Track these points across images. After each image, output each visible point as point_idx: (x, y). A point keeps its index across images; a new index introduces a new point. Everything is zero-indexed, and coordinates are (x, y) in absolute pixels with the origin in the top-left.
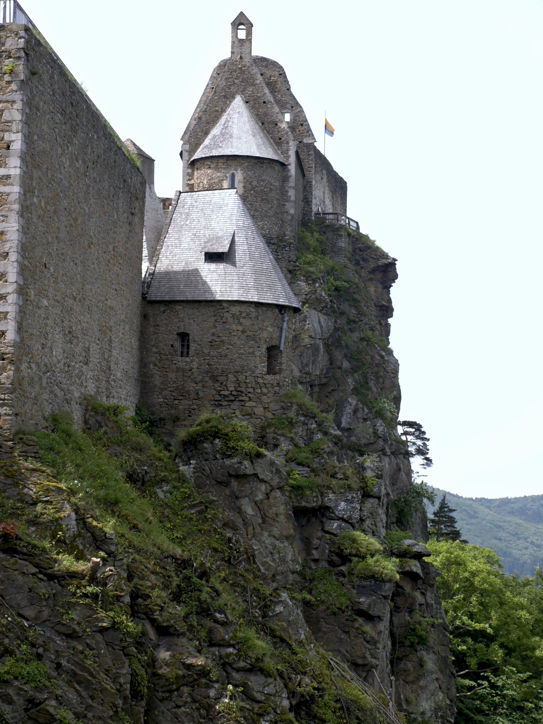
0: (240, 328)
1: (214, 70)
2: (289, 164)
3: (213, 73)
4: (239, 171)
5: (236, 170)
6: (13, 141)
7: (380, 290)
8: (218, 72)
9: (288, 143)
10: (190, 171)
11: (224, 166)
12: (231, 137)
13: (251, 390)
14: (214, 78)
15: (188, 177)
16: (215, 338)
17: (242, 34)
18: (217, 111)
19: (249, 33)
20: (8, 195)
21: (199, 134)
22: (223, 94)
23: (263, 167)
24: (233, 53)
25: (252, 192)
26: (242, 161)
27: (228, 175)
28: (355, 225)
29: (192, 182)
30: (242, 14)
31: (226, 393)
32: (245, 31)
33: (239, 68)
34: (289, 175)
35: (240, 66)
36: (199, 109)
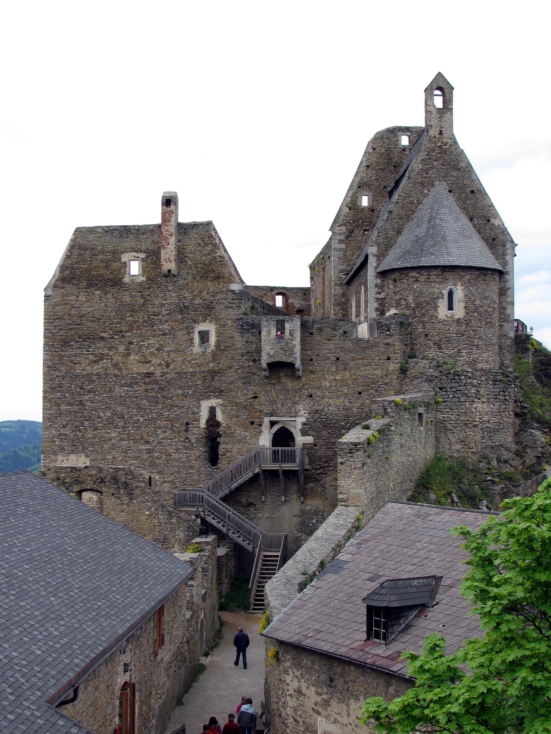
1: (369, 143)
3: (367, 148)
4: (459, 287)
5: (455, 285)
8: (374, 147)
9: (504, 245)
10: (379, 281)
11: (439, 280)
12: (444, 239)
14: (369, 153)
17: (438, 102)
18: (412, 203)
21: (391, 232)
22: (420, 180)
23: (485, 280)
25: (475, 314)
26: (462, 274)
27: (444, 292)
29: (382, 295)
30: (440, 75)
32: (441, 98)
33: (439, 147)
34: (507, 286)
35: (439, 144)
36: (351, 192)
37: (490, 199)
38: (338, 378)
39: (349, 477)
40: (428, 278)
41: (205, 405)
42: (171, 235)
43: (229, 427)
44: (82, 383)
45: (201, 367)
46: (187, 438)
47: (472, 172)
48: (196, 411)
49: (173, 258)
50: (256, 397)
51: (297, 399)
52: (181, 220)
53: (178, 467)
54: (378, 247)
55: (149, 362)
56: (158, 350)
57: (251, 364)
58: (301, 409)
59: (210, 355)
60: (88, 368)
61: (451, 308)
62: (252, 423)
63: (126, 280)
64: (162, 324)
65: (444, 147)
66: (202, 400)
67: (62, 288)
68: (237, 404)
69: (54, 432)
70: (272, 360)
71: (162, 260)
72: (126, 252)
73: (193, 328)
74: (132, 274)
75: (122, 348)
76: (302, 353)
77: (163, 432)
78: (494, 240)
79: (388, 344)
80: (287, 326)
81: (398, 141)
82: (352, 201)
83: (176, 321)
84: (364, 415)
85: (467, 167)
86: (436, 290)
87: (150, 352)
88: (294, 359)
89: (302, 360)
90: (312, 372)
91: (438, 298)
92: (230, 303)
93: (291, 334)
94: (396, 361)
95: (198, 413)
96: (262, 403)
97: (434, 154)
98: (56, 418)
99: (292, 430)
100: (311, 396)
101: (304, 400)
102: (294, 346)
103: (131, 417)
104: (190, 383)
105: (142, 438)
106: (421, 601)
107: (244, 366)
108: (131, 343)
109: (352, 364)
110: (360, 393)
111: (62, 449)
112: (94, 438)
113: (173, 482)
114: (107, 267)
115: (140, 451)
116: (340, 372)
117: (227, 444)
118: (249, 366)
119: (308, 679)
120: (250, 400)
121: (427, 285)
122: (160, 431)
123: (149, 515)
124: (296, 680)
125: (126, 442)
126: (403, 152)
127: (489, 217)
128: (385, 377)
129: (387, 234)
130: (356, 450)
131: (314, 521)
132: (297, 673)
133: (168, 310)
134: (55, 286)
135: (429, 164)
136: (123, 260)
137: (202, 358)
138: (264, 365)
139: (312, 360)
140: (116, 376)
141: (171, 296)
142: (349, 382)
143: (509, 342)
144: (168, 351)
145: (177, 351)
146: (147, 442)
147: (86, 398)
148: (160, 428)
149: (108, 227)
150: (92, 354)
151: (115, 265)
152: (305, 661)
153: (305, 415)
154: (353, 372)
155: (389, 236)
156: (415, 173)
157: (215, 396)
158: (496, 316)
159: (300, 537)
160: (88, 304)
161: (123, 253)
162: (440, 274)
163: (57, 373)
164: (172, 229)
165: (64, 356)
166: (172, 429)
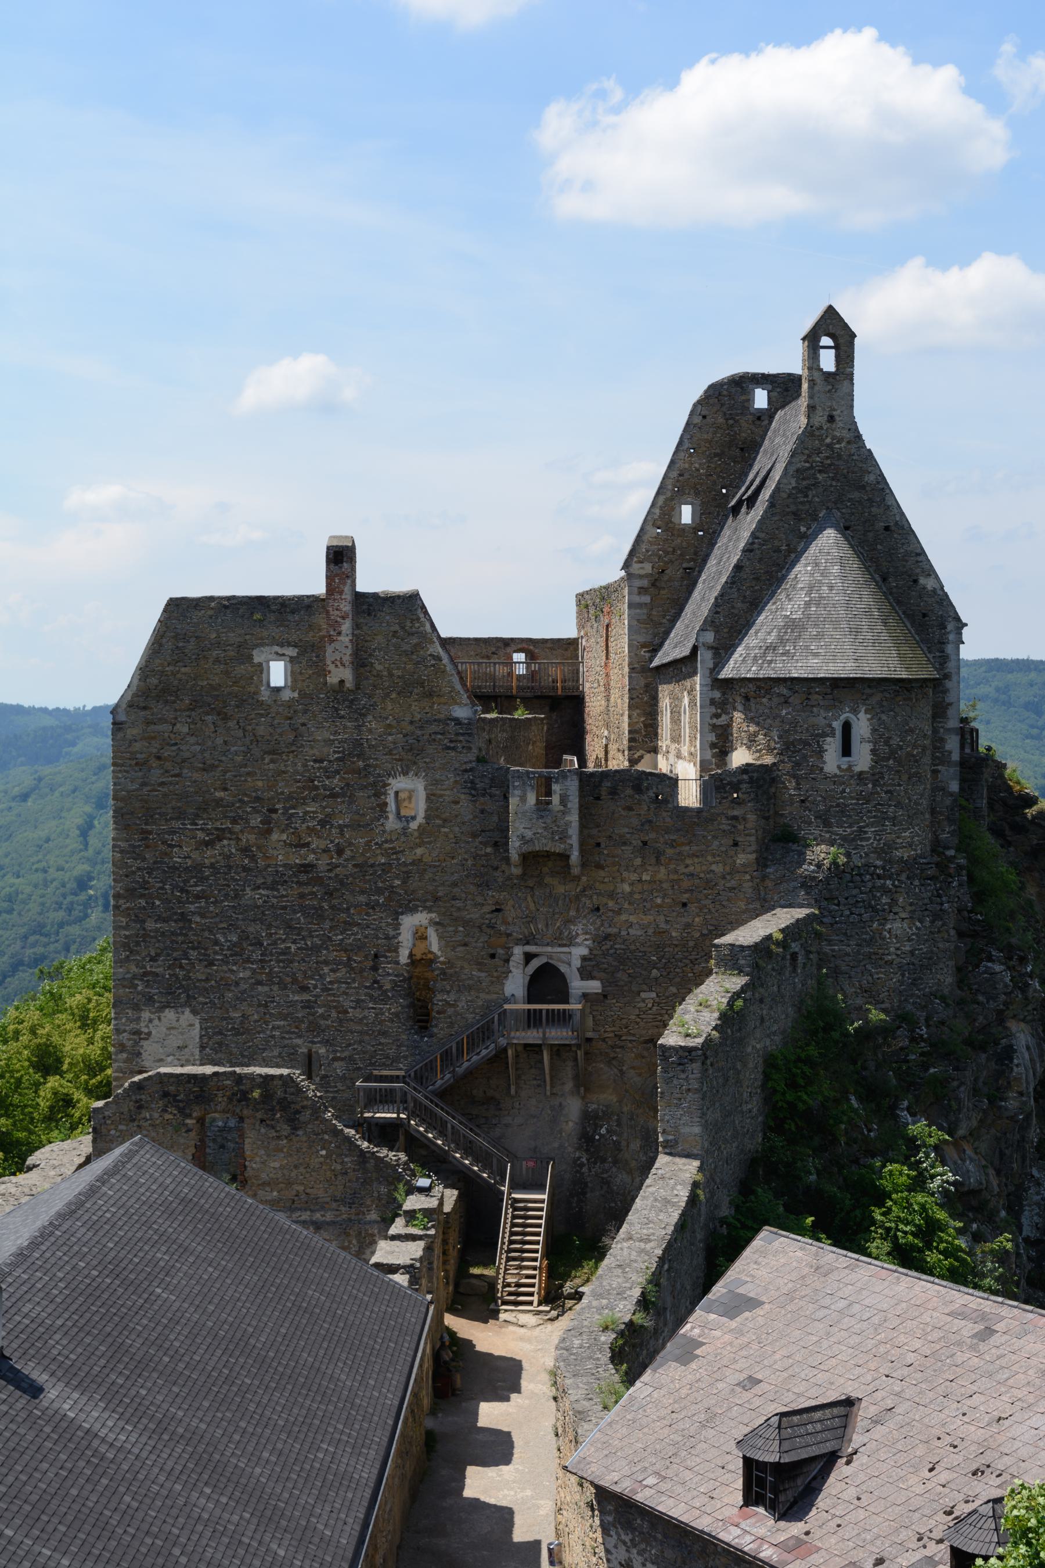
1: (695, 405)
4: (862, 715)
5: (855, 711)
8: (703, 413)
10: (717, 695)
15: (713, 710)
17: (828, 361)
22: (793, 508)
23: (910, 699)
25: (891, 762)
26: (868, 691)
27: (835, 724)
32: (833, 351)
34: (947, 700)
35: (828, 440)
36: (662, 498)
37: (919, 542)
38: (646, 877)
39: (678, 1106)
40: (807, 699)
41: (410, 922)
42: (343, 618)
43: (449, 963)
44: (185, 882)
45: (400, 856)
46: (376, 982)
47: (888, 491)
48: (392, 933)
49: (347, 659)
50: (498, 910)
51: (572, 913)
52: (361, 588)
53: (361, 1033)
54: (717, 632)
55: (307, 845)
56: (323, 823)
57: (489, 850)
58: (579, 932)
59: (416, 834)
60: (195, 855)
61: (846, 751)
62: (493, 956)
63: (265, 695)
64: (328, 778)
65: (837, 446)
66: (402, 913)
67: (145, 708)
68: (466, 923)
69: (134, 969)
70: (525, 849)
71: (328, 662)
72: (263, 645)
73: (386, 785)
74: (272, 684)
75: (256, 821)
76: (581, 832)
77: (333, 971)
78: (924, 615)
79: (735, 818)
80: (556, 787)
81: (748, 400)
82: (663, 514)
83: (353, 771)
84: (691, 944)
85: (878, 483)
86: (821, 721)
87: (308, 827)
88: (568, 847)
89: (582, 844)
90: (600, 867)
91: (825, 735)
92: (451, 741)
93: (564, 800)
94: (749, 849)
95: (395, 937)
96: (510, 919)
97: (818, 459)
98: (138, 944)
99: (563, 968)
100: (598, 909)
101: (585, 916)
102: (568, 824)
103: (275, 943)
104: (380, 885)
105: (295, 981)
106: (828, 1447)
107: (478, 855)
108: (275, 811)
109: (670, 852)
110: (684, 905)
111: (150, 1000)
112: (207, 980)
113: (350, 1059)
114: (227, 673)
115: (292, 1004)
116: (649, 868)
117: (448, 992)
118: (487, 854)
119: (644, 1550)
120: (487, 916)
121: (804, 712)
122: (326, 970)
123: (326, 1157)
124: (622, 1549)
125: (266, 988)
126: (758, 422)
127: (917, 575)
128: (728, 877)
129: (733, 607)
130: (691, 1060)
131: (603, 1131)
132: (623, 1537)
133: (339, 752)
134: (130, 705)
135: (808, 479)
136: (256, 660)
137: (403, 839)
138: (514, 855)
139: (598, 845)
140: (245, 869)
141: (345, 727)
142: (665, 886)
143: (948, 801)
144: (341, 828)
145: (356, 826)
146: (304, 989)
147: (192, 908)
148: (326, 963)
149: (229, 598)
150: (202, 829)
151: (241, 670)
152: (639, 1521)
153: (587, 943)
154: (672, 866)
155: (736, 611)
156: (784, 495)
157: (425, 908)
158: (927, 760)
159: (579, 1158)
160: (192, 740)
161: (257, 646)
162: (829, 691)
163: (138, 863)
164: (346, 607)
165: (150, 833)
166: (348, 964)
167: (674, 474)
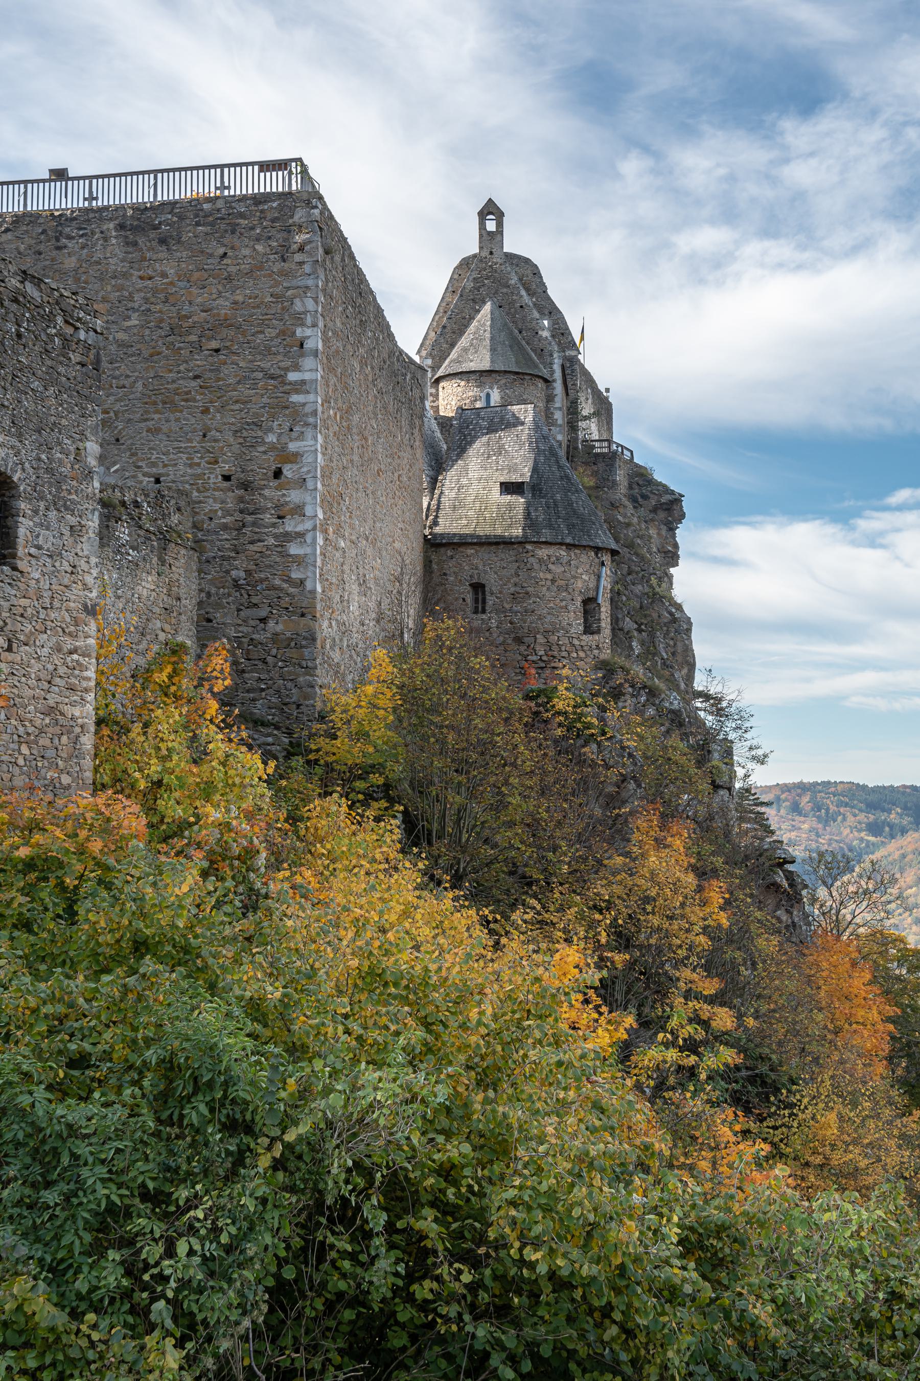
0: (549, 576)
2: (554, 381)
5: (492, 388)
6: (309, 337)
7: (664, 532)
9: (551, 355)
13: (564, 654)
16: (518, 589)
17: (491, 226)
19: (500, 224)
20: (304, 404)
24: (481, 248)
28: (629, 454)
31: (535, 658)
167: (444, 304)
